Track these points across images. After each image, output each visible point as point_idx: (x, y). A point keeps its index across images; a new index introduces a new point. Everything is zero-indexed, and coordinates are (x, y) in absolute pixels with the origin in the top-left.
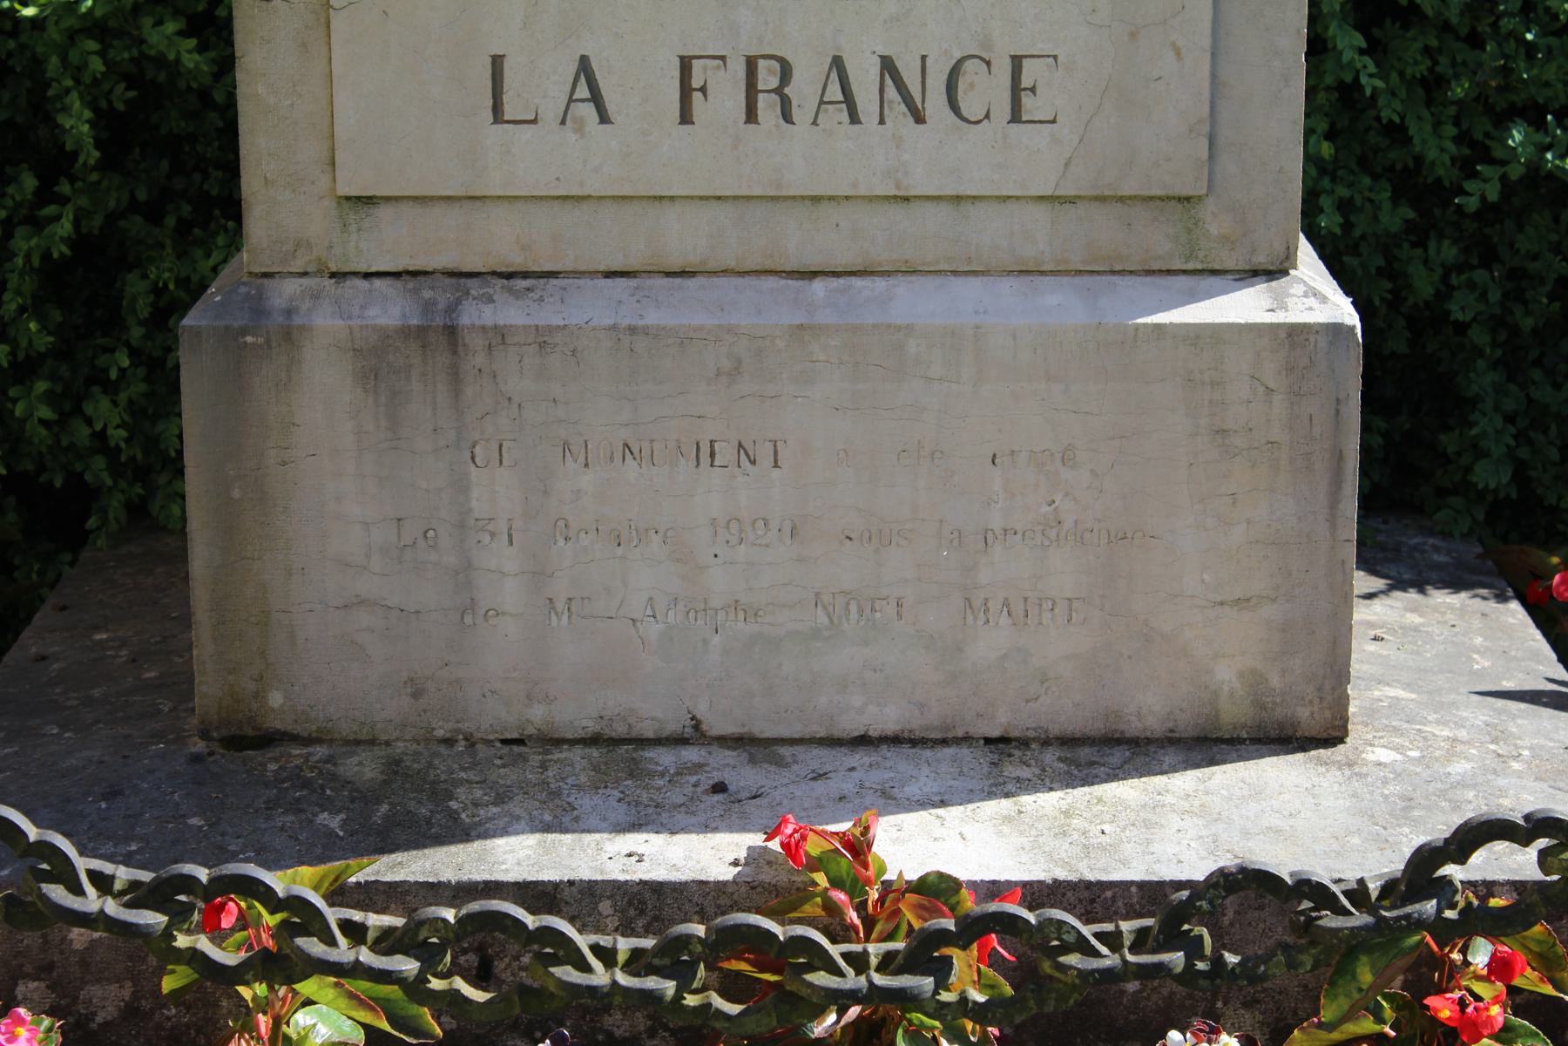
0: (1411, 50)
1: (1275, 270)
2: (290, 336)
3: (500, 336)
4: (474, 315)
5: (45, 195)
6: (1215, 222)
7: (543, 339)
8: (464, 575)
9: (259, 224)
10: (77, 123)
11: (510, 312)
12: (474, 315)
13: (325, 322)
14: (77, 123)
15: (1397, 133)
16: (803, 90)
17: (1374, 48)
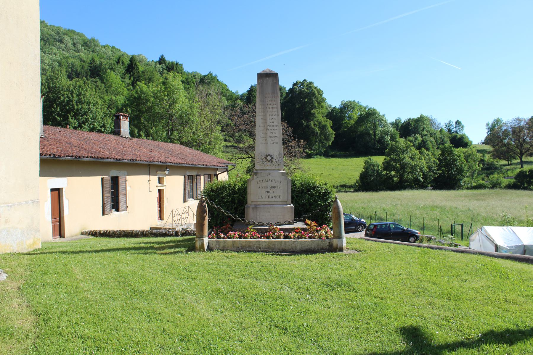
0: (299, 198)
1: (291, 204)
2: (249, 207)
3: (258, 207)
4: (257, 206)
5: (235, 204)
6: (288, 202)
7: (260, 207)
8: (257, 217)
9: (248, 203)
10: (236, 201)
11: (259, 206)
12: (257, 206)
13: (251, 207)
14: (236, 201)
15: (298, 202)
16: (271, 197)
17: (297, 198)
